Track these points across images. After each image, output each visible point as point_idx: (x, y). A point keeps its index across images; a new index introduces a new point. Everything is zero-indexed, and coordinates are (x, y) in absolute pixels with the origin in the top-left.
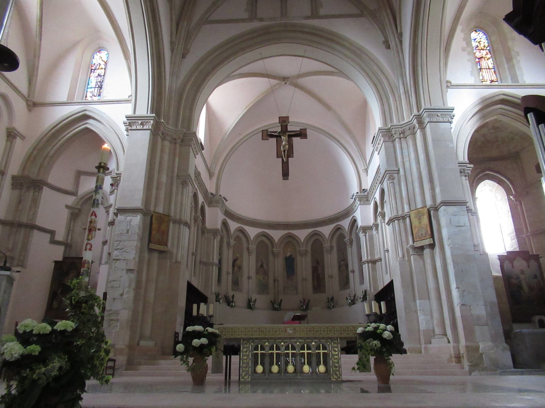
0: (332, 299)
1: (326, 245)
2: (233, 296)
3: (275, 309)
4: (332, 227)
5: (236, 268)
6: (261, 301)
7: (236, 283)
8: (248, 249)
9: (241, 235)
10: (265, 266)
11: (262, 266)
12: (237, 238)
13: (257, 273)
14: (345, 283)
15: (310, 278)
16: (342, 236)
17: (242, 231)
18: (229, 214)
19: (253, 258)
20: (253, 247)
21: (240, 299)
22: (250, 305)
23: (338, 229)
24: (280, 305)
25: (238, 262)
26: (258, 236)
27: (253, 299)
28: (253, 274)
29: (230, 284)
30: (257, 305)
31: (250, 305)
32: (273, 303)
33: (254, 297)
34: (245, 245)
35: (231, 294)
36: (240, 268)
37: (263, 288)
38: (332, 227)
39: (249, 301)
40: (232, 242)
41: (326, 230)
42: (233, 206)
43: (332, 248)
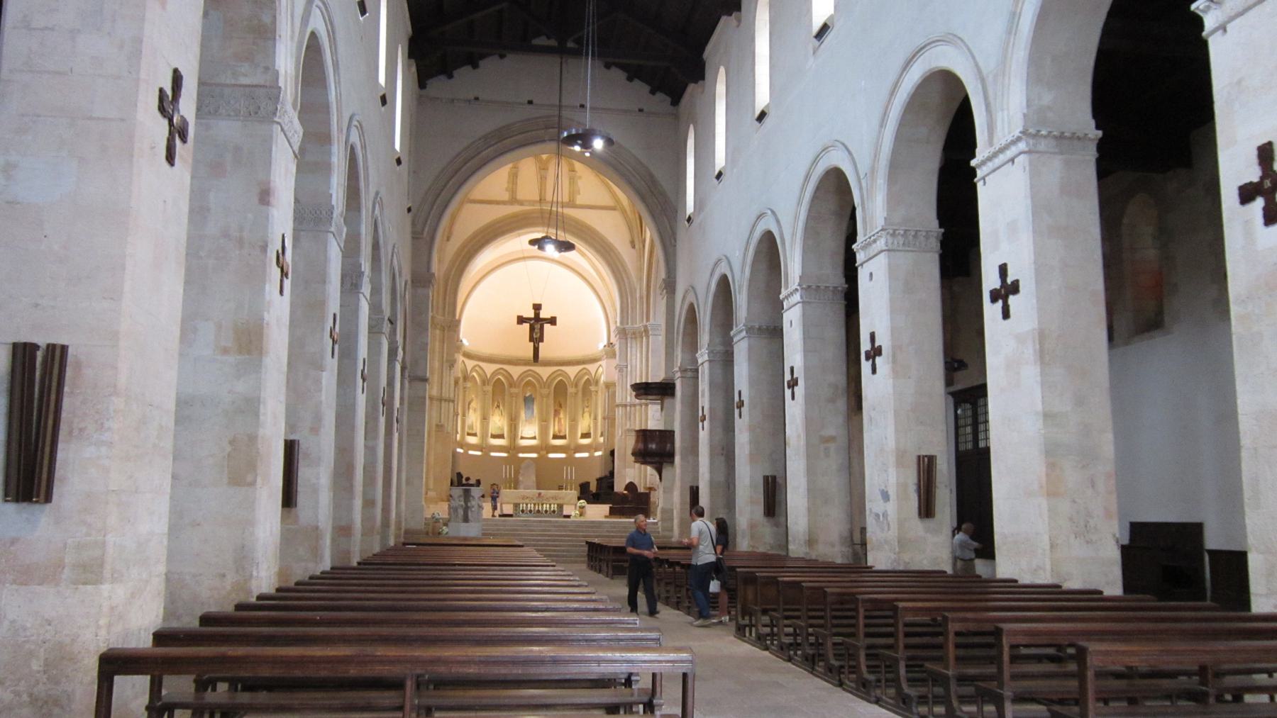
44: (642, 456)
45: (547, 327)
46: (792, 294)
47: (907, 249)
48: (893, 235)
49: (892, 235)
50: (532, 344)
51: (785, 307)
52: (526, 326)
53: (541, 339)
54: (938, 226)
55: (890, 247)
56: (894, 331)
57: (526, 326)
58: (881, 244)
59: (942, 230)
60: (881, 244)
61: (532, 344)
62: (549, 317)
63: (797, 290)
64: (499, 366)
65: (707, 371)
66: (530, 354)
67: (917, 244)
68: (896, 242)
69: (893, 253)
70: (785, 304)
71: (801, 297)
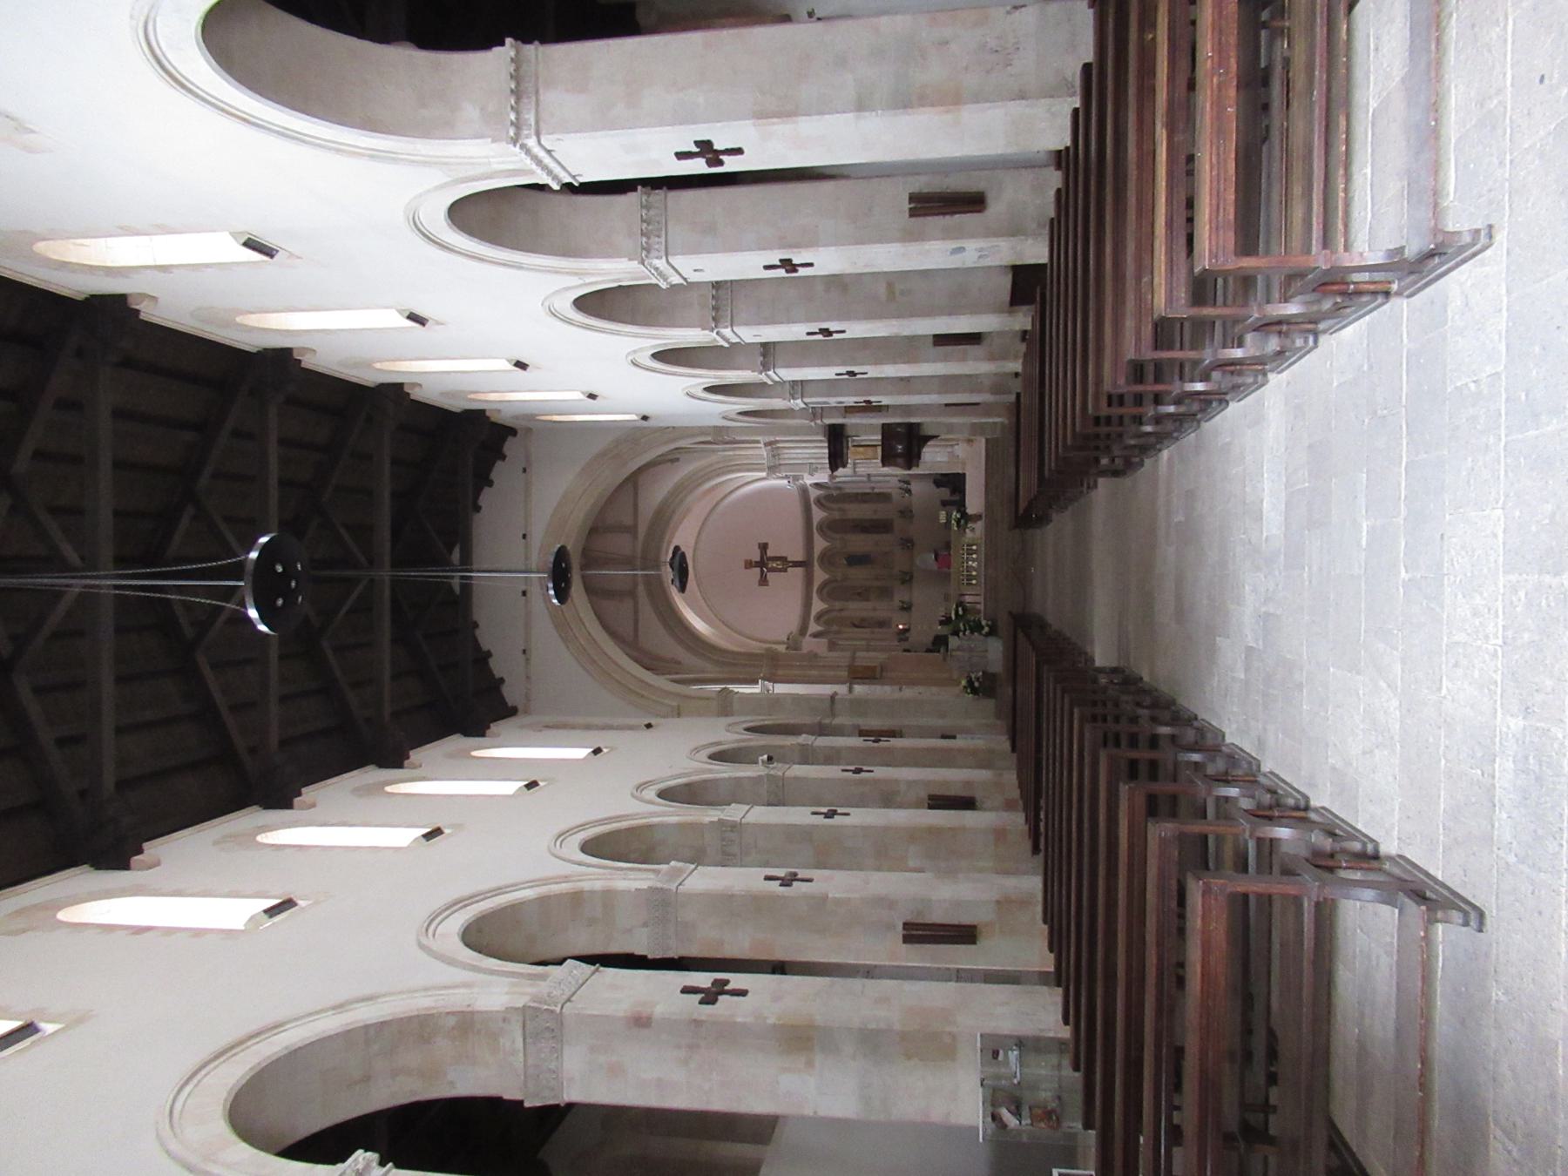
0: (901, 512)
1: (837, 515)
4: (815, 509)
6: (900, 595)
7: (882, 624)
8: (841, 610)
9: (826, 617)
10: (859, 591)
11: (859, 594)
12: (827, 623)
13: (867, 600)
14: (884, 497)
15: (876, 537)
16: (829, 498)
17: (818, 618)
18: (803, 630)
20: (838, 605)
22: (906, 608)
23: (819, 502)
24: (906, 573)
25: (856, 623)
28: (869, 605)
29: (884, 630)
30: (906, 599)
31: (906, 608)
32: (903, 582)
33: (896, 602)
34: (834, 614)
36: (863, 620)
37: (885, 593)
38: (815, 509)
39: (903, 609)
40: (835, 628)
41: (818, 515)
42: (793, 624)
43: (840, 510)
44: (911, 458)
45: (770, 553)
46: (724, 338)
47: (663, 232)
48: (648, 249)
49: (648, 251)
50: (789, 569)
51: (738, 340)
52: (770, 576)
53: (783, 559)
54: (634, 194)
55: (663, 253)
56: (762, 246)
57: (770, 576)
58: (661, 263)
59: (639, 187)
60: (661, 263)
61: (789, 569)
62: (759, 551)
63: (718, 333)
64: (815, 595)
65: (814, 400)
66: (799, 571)
67: (657, 219)
68: (657, 247)
69: (669, 250)
70: (734, 341)
71: (726, 327)
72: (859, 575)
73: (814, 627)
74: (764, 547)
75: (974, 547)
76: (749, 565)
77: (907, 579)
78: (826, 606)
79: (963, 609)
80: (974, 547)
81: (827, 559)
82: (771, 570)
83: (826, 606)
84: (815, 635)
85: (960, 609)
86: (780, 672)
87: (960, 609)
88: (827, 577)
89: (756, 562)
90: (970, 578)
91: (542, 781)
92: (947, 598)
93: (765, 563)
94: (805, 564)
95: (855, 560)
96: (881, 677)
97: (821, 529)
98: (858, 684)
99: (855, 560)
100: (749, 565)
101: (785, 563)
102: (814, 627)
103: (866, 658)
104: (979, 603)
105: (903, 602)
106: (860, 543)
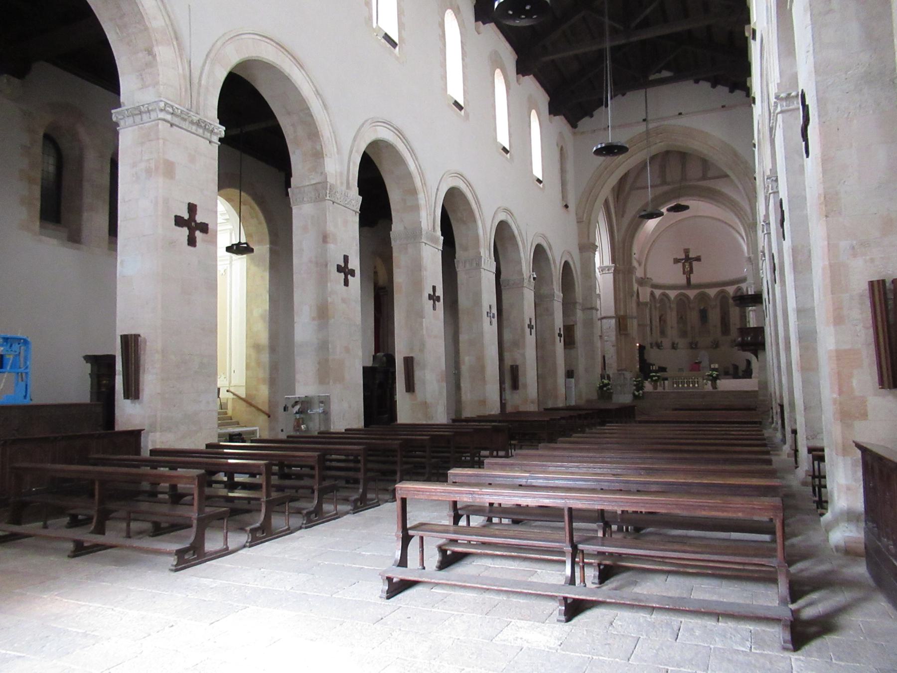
2: (661, 342)
3: (692, 348)
5: (662, 322)
6: (682, 343)
7: (663, 333)
8: (670, 307)
10: (684, 317)
11: (681, 318)
12: (662, 300)
13: (678, 323)
15: (719, 324)
17: (664, 294)
19: (674, 313)
20: (674, 306)
21: (667, 343)
22: (674, 346)
24: (696, 345)
25: (663, 317)
26: (677, 296)
27: (676, 342)
29: (659, 334)
30: (679, 346)
31: (674, 346)
32: (691, 344)
33: (677, 340)
35: (659, 341)
36: (665, 321)
37: (683, 334)
39: (673, 344)
42: (656, 280)
72: (693, 317)
73: (658, 293)
74: (698, 259)
75: (696, 385)
76: (687, 251)
77: (693, 346)
78: (672, 299)
79: (656, 380)
80: (696, 385)
81: (703, 297)
82: (684, 264)
83: (672, 299)
84: (652, 294)
85: (656, 378)
86: (621, 276)
87: (656, 378)
88: (692, 298)
89: (688, 255)
90: (677, 383)
91: (510, 155)
92: (681, 370)
93: (688, 261)
94: (689, 286)
95: (704, 315)
96: (620, 334)
97: (723, 291)
98: (616, 321)
99: (704, 315)
100: (687, 251)
101: (689, 273)
102: (658, 293)
103: (633, 326)
104: (664, 389)
105: (677, 344)
106: (714, 316)
